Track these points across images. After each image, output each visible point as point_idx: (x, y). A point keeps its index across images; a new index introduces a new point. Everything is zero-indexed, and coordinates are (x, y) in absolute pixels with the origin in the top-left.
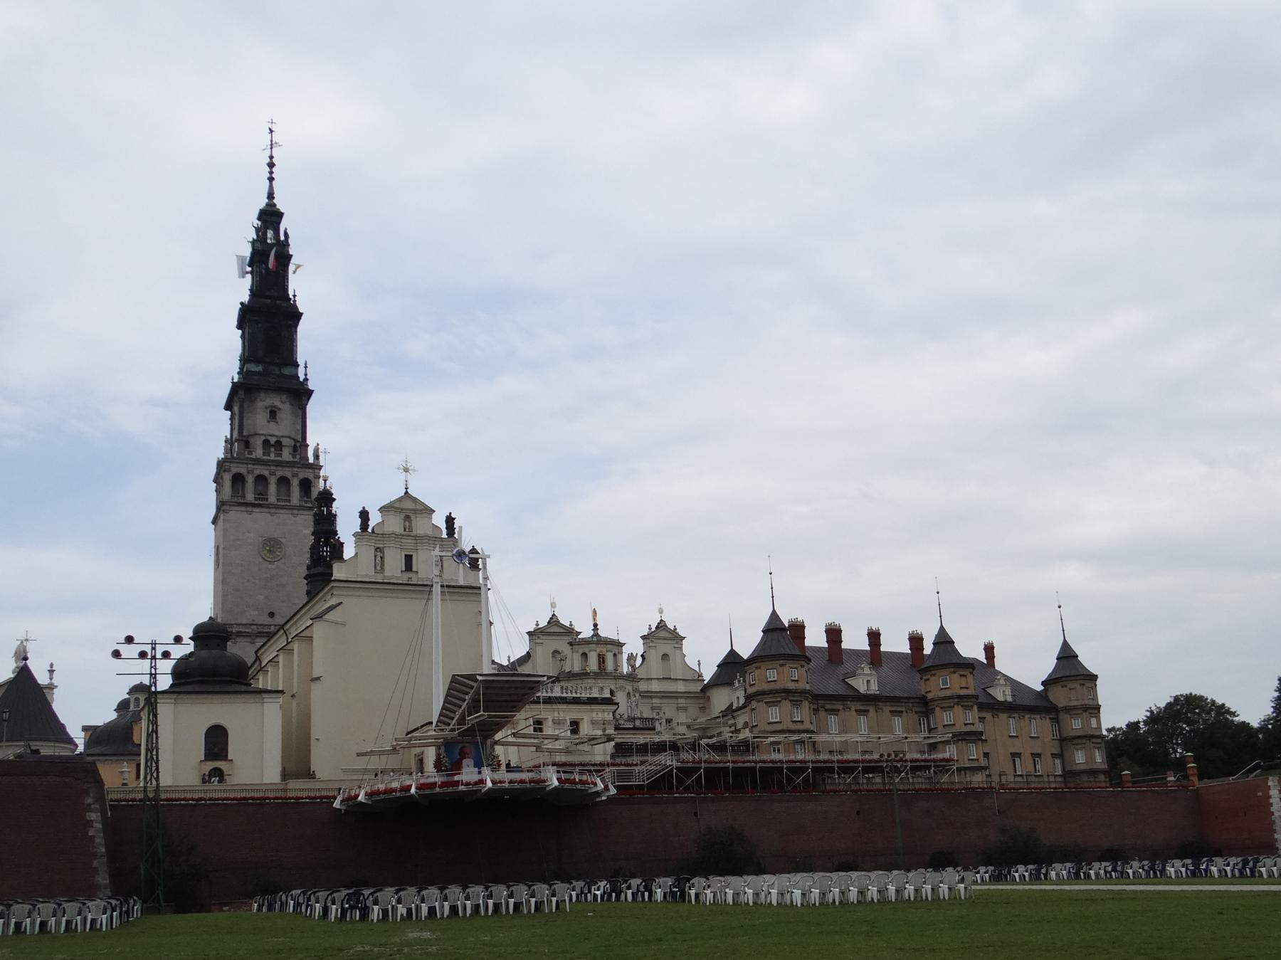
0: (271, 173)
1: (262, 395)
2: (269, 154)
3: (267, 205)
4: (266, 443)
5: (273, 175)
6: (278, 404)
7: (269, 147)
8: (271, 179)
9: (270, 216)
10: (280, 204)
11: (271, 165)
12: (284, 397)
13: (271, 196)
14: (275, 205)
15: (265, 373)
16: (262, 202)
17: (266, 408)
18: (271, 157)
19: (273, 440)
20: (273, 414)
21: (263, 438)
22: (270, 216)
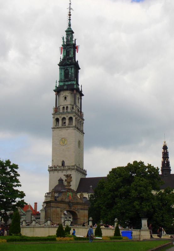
0: (70, 17)
1: (62, 93)
2: (68, 12)
3: (68, 29)
4: (64, 108)
5: (71, 18)
6: (67, 94)
7: (69, 9)
8: (70, 20)
9: (70, 32)
10: (73, 28)
11: (70, 15)
12: (69, 92)
13: (70, 25)
14: (71, 28)
15: (64, 85)
16: (66, 27)
17: (64, 96)
18: (70, 12)
19: (65, 107)
20: (65, 98)
21: (63, 106)
22: (70, 32)
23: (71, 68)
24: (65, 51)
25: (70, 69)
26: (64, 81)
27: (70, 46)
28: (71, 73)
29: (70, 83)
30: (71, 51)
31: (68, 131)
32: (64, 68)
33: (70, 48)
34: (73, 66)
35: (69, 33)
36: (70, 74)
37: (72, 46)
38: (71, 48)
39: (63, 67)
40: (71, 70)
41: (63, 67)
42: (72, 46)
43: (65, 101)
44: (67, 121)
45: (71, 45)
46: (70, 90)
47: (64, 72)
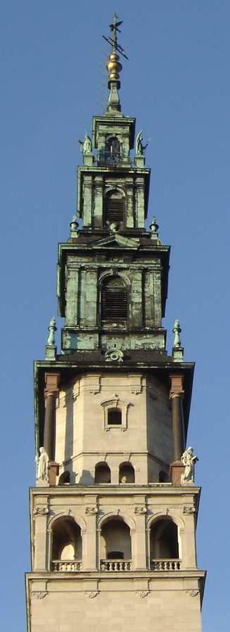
17: (104, 404)
20: (114, 417)
23: (145, 272)
24: (99, 200)
25: (139, 276)
26: (101, 333)
27: (130, 180)
28: (143, 297)
29: (139, 343)
30: (134, 201)
31: (151, 600)
32: (100, 270)
33: (127, 187)
34: (153, 263)
35: (118, 130)
36: (137, 299)
37: (140, 180)
38: (135, 188)
39: (96, 265)
40: (144, 280)
41: (96, 265)
42: (140, 180)
43: (116, 430)
44: (139, 544)
45: (135, 176)
46: (145, 373)
47: (102, 287)
